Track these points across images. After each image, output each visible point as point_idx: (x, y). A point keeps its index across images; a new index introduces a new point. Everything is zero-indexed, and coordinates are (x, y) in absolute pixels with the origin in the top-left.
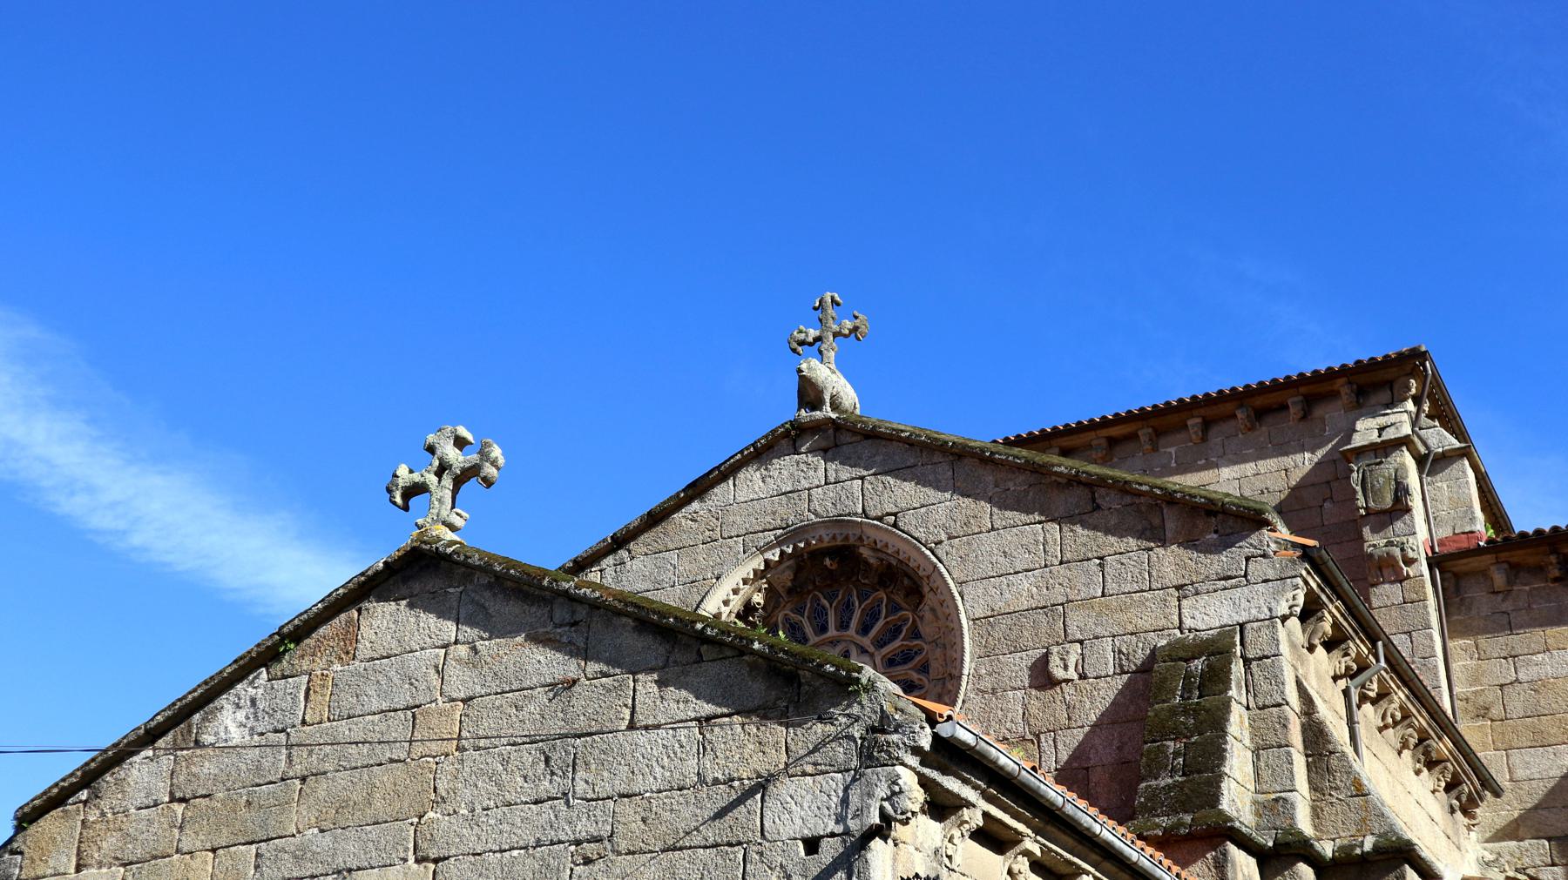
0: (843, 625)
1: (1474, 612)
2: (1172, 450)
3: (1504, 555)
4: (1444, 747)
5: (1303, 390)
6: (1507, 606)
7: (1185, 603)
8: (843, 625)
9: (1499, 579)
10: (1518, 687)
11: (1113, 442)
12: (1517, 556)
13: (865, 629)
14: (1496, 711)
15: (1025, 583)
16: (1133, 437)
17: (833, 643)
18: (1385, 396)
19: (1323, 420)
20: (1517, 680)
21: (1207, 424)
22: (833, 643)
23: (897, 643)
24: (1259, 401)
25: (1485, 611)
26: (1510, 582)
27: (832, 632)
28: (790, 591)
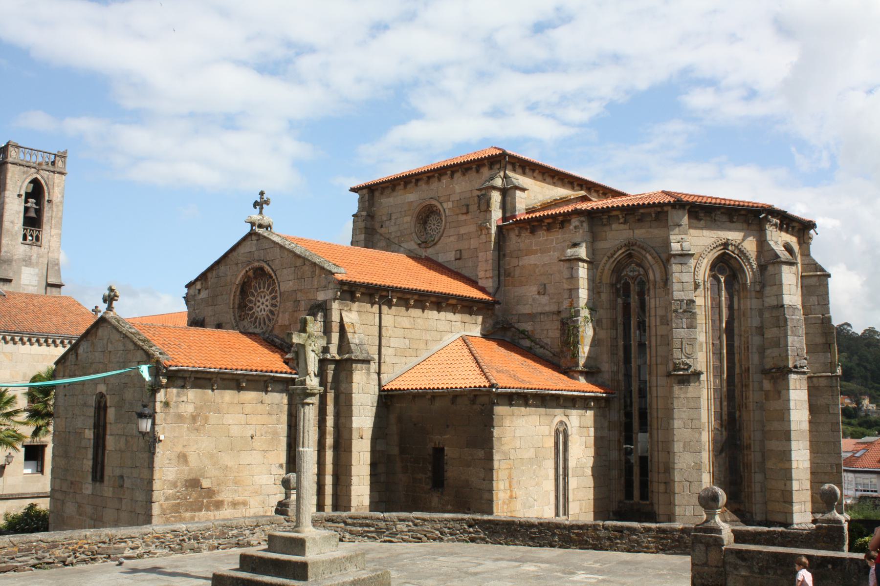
0: (264, 288)
2: (444, 181)
3: (517, 225)
4: (454, 302)
5: (476, 163)
6: (519, 241)
7: (318, 293)
8: (264, 288)
9: (517, 232)
10: (518, 267)
11: (429, 178)
12: (521, 225)
13: (268, 290)
14: (512, 274)
15: (291, 283)
16: (433, 176)
17: (263, 292)
18: (498, 166)
19: (482, 173)
21: (453, 173)
22: (263, 292)
23: (273, 294)
24: (465, 166)
26: (520, 233)
27: (262, 290)
28: (254, 278)
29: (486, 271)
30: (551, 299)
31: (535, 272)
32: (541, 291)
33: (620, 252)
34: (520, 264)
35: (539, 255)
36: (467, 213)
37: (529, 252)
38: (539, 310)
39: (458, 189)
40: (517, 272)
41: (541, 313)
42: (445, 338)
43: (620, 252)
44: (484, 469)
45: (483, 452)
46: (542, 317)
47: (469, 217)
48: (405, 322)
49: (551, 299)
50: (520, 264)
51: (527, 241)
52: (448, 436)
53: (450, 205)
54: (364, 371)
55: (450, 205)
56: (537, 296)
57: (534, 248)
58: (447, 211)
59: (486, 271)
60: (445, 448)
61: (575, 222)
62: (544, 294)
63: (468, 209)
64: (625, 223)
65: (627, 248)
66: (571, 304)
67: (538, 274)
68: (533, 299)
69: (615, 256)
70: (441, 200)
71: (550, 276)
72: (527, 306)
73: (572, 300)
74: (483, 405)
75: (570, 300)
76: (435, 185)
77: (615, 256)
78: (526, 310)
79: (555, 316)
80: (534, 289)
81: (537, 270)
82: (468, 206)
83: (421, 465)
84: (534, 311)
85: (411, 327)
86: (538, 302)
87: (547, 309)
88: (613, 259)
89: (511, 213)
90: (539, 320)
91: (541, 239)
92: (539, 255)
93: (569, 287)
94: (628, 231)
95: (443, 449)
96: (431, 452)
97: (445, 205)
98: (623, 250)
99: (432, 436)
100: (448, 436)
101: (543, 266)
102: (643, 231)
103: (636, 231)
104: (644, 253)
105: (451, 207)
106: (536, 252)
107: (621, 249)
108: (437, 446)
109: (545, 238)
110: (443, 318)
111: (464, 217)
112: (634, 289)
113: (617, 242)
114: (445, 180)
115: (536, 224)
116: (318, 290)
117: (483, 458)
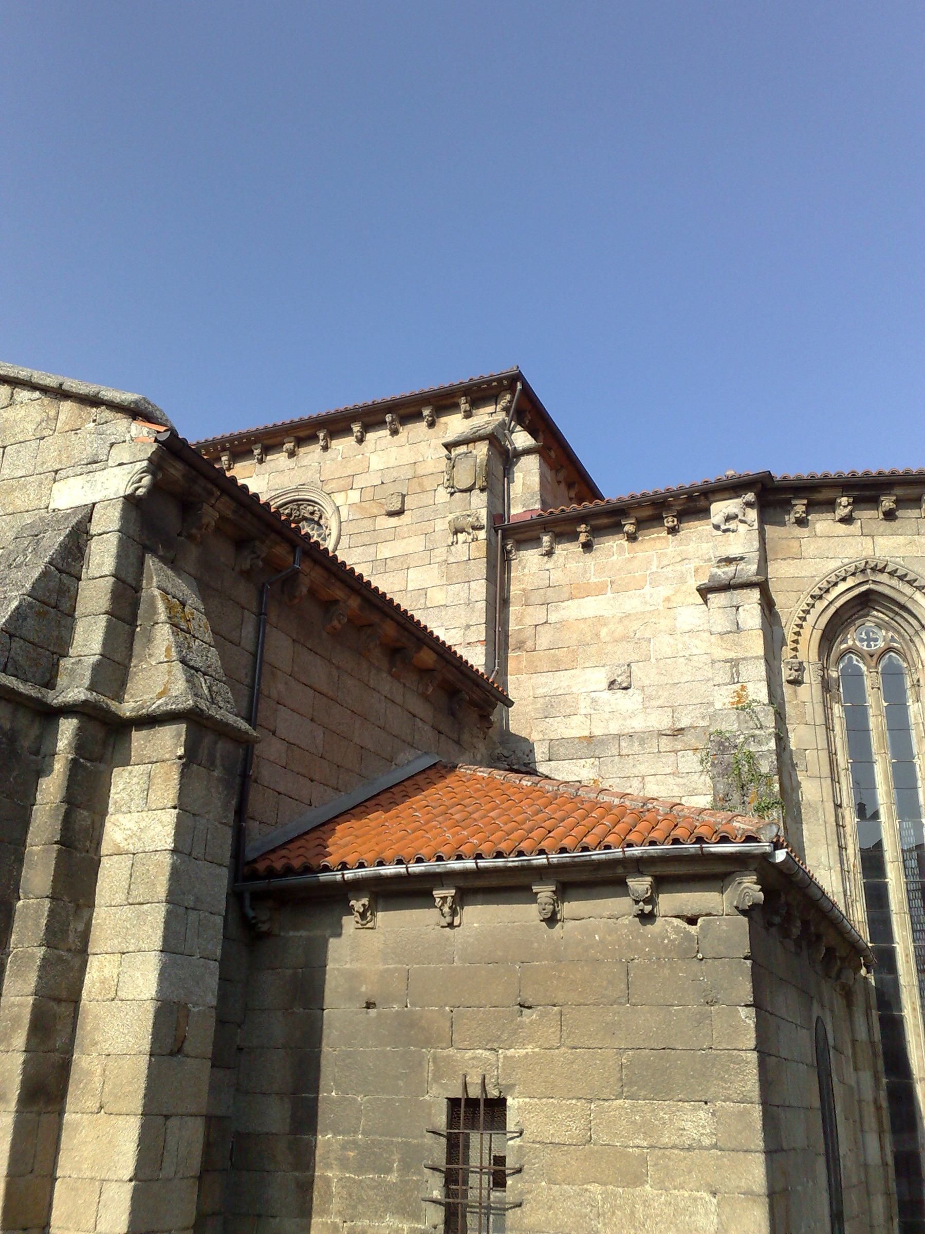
1: (526, 571)
2: (340, 447)
4: (427, 657)
10: (547, 626)
14: (529, 644)
20: (546, 622)
25: (534, 569)
29: (468, 627)
30: (648, 698)
31: (597, 635)
32: (619, 679)
33: (842, 587)
34: (553, 618)
35: (609, 595)
36: (400, 513)
37: (578, 591)
38: (614, 729)
39: (377, 462)
40: (545, 639)
41: (619, 736)
42: (402, 757)
43: (842, 587)
44: (714, 1194)
45: (703, 1115)
46: (623, 744)
47: (405, 518)
48: (319, 673)
49: (650, 698)
50: (553, 618)
51: (572, 565)
52: (529, 1049)
53: (354, 496)
54: (216, 774)
55: (354, 496)
56: (607, 695)
57: (593, 580)
58: (344, 512)
59: (468, 627)
60: (510, 1101)
61: (720, 509)
62: (625, 688)
63: (403, 502)
64: (847, 520)
65: (860, 578)
66: (740, 696)
67: (608, 639)
68: (594, 701)
69: (831, 597)
70: (327, 488)
71: (644, 644)
72: (575, 720)
73: (743, 688)
74: (692, 921)
75: (737, 687)
76: (311, 454)
77: (831, 597)
78: (575, 728)
79: (664, 740)
80: (600, 678)
81: (604, 632)
82: (404, 496)
83: (393, 1178)
84: (597, 732)
85: (330, 694)
86: (608, 709)
87: (638, 724)
88: (826, 603)
89: (524, 506)
90: (616, 752)
91: (615, 557)
92: (609, 595)
93: (732, 655)
94: (859, 539)
95: (497, 1107)
96: (441, 1120)
97: (339, 499)
98: (850, 582)
99: (452, 1051)
100: (529, 1049)
101: (621, 620)
102: (901, 539)
103: (880, 540)
104: (908, 590)
105: (357, 500)
106: (600, 590)
107: (844, 579)
108: (474, 1092)
109: (627, 555)
110: (399, 699)
111: (394, 521)
112: (871, 680)
113: (833, 565)
114: (343, 445)
115: (604, 521)
116: (62, 474)
117: (706, 1141)
